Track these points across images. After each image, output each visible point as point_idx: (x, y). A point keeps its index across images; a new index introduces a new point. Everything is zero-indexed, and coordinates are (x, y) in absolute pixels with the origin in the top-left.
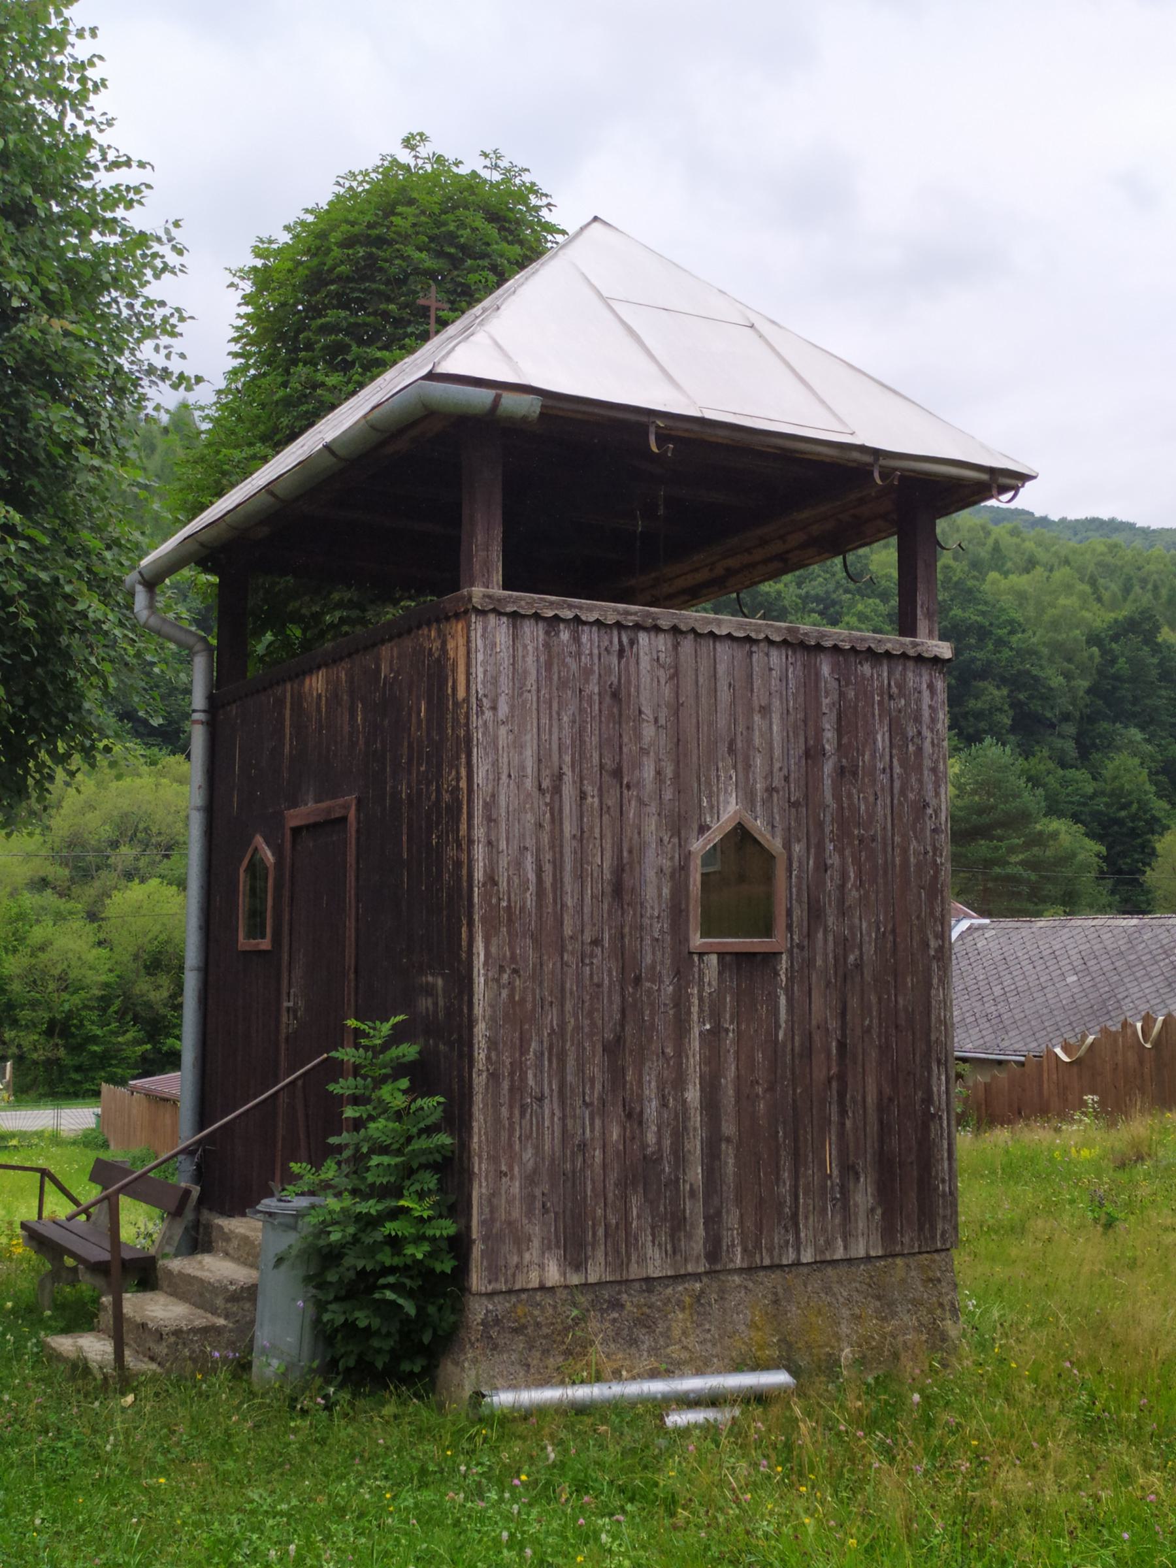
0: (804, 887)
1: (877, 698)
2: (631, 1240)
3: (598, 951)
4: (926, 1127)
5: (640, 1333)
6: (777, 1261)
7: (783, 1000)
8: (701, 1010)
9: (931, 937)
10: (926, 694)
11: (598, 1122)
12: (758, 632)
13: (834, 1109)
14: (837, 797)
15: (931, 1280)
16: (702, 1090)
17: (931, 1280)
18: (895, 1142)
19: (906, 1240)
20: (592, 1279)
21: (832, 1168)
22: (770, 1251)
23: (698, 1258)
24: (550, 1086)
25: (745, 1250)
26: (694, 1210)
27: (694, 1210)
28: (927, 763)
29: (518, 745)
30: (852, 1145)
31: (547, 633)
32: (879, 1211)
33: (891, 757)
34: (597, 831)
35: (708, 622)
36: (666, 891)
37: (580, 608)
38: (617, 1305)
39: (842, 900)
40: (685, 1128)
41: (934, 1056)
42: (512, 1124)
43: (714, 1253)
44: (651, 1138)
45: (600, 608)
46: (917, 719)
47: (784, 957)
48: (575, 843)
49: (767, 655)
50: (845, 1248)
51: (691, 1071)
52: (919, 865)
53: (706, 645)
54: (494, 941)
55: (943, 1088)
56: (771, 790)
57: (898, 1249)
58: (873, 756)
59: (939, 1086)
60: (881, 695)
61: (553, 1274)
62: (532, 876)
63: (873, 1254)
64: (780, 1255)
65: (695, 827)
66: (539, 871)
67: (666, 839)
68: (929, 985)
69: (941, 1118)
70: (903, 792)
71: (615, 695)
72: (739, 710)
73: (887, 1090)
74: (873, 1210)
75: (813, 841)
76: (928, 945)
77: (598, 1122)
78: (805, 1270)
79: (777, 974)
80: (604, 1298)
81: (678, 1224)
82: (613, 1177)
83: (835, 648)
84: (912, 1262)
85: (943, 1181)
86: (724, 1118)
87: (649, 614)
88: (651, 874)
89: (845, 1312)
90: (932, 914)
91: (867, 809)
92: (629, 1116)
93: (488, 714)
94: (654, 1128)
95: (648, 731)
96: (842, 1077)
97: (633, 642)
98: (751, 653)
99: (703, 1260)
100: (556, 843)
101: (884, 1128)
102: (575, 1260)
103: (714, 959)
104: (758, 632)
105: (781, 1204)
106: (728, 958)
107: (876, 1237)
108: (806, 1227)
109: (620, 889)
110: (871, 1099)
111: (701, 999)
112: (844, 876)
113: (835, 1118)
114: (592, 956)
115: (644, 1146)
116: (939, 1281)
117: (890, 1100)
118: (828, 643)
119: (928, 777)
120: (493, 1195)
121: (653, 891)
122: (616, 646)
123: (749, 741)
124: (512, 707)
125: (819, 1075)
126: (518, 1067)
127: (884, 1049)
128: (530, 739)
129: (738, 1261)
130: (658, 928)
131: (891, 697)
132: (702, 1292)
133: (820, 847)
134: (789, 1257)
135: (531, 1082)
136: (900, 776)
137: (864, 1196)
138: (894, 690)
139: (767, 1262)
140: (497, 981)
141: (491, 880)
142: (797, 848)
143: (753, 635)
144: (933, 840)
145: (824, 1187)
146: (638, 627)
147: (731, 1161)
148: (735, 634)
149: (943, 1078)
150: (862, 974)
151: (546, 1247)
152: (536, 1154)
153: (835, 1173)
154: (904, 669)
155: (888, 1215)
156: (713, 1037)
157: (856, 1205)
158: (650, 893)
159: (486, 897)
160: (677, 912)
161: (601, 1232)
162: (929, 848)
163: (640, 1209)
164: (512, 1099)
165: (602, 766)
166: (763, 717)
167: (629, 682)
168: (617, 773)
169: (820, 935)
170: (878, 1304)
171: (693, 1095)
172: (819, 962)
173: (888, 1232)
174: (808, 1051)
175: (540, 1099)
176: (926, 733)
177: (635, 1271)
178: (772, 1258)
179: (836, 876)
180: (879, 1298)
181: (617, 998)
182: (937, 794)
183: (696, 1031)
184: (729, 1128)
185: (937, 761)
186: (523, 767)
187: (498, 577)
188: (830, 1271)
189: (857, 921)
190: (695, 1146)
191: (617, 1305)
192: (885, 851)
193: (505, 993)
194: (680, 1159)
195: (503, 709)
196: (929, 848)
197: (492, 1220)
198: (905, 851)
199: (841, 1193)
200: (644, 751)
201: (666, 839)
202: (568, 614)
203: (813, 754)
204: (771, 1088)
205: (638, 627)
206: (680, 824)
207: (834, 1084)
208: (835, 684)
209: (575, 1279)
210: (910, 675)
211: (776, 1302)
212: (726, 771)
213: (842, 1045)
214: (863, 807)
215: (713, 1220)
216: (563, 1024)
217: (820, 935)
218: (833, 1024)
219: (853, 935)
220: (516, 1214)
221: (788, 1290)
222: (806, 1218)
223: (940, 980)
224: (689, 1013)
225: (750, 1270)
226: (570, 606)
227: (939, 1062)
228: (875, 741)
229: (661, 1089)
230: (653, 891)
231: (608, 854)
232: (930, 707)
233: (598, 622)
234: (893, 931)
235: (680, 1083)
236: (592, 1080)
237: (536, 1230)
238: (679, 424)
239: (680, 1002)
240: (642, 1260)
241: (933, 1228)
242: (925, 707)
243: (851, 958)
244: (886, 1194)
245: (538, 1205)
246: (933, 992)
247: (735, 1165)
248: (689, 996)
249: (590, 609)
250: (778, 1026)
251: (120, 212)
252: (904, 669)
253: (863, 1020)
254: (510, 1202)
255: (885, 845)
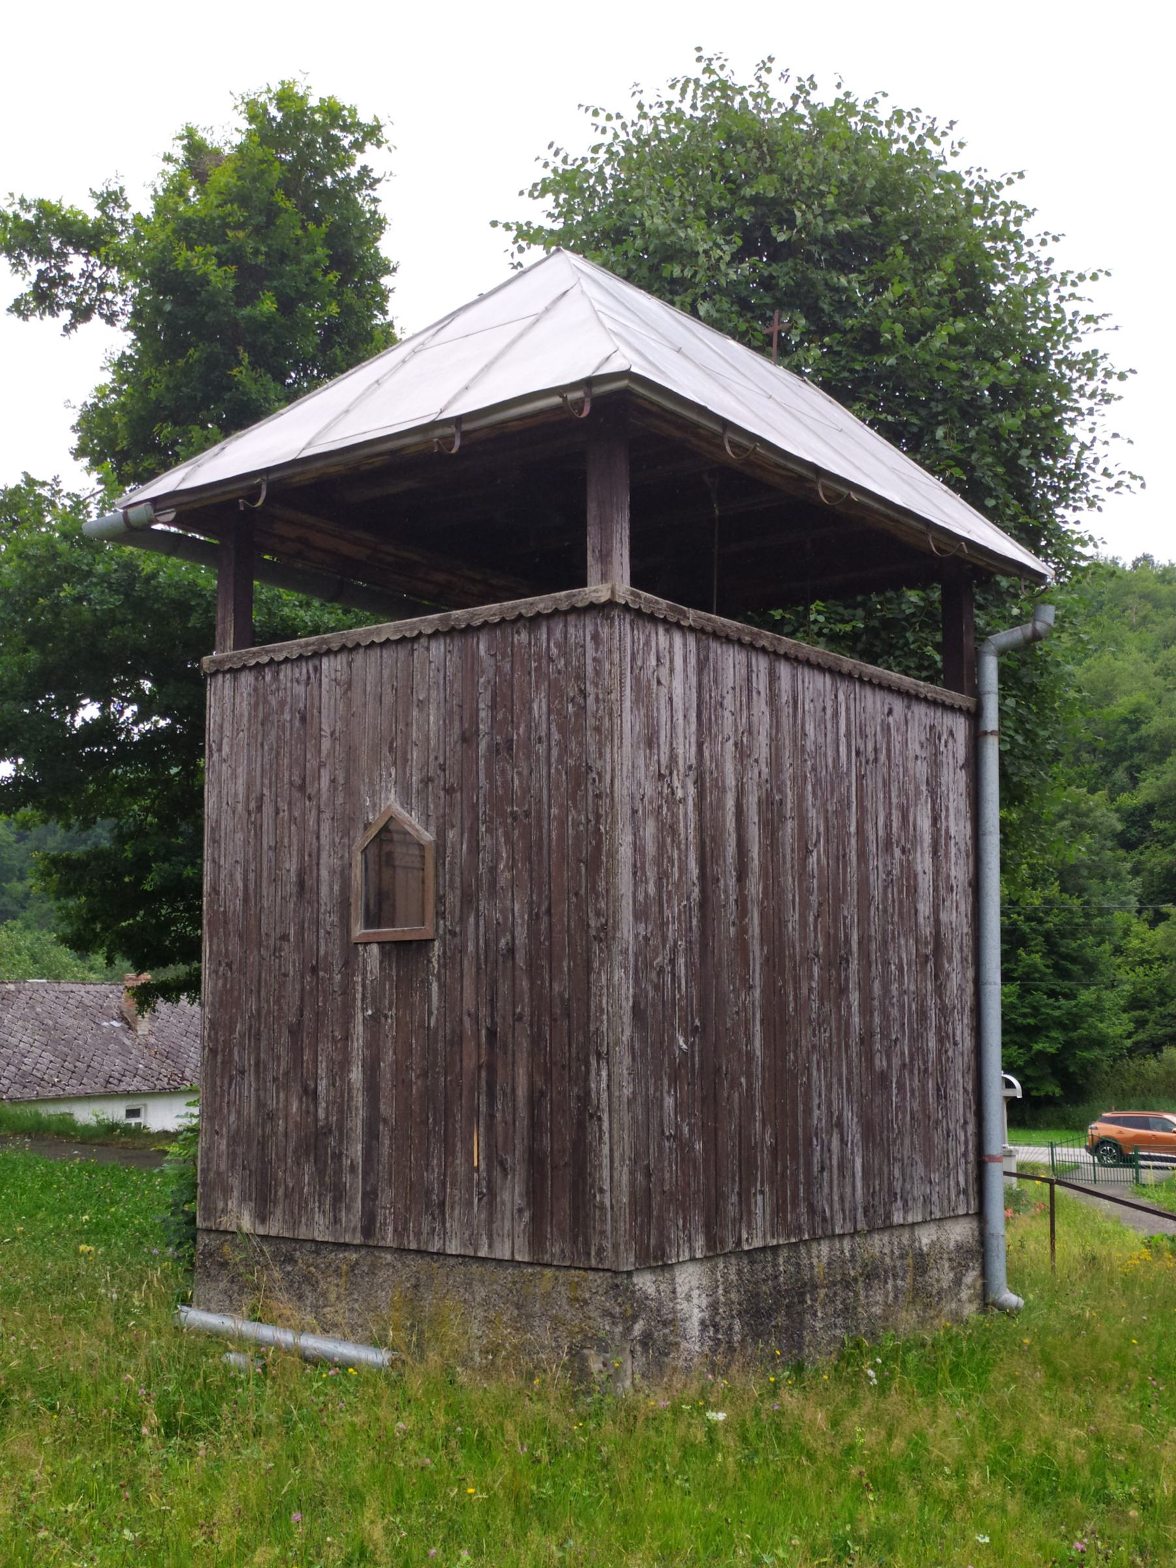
0: (457, 872)
1: (534, 664)
2: (303, 1206)
3: (285, 945)
4: (581, 1127)
5: (306, 1289)
6: (423, 1247)
7: (435, 987)
8: (364, 998)
9: (591, 915)
10: (590, 645)
11: (282, 1095)
12: (411, 630)
13: (483, 1099)
14: (490, 776)
15: (577, 1300)
16: (364, 1072)
17: (577, 1300)
18: (547, 1140)
19: (556, 1249)
20: (273, 1233)
21: (478, 1158)
22: (418, 1234)
23: (354, 1229)
24: (249, 1061)
25: (395, 1230)
26: (355, 1185)
27: (355, 1185)
28: (591, 722)
29: (234, 776)
30: (500, 1139)
31: (256, 679)
32: (527, 1215)
33: (549, 724)
34: (286, 840)
35: (370, 633)
36: (336, 888)
37: (273, 651)
38: (291, 1260)
39: (493, 883)
40: (349, 1107)
41: (592, 1048)
42: (222, 1091)
43: (368, 1229)
44: (321, 1114)
45: (287, 647)
46: (580, 677)
47: (436, 944)
48: (271, 853)
49: (428, 649)
50: (490, 1246)
51: (355, 1053)
52: (578, 837)
53: (375, 654)
54: (215, 940)
55: (604, 1085)
56: (427, 781)
57: (547, 1258)
58: (529, 728)
59: (599, 1082)
60: (539, 661)
61: (246, 1224)
62: (240, 885)
63: (518, 1258)
64: (427, 1243)
65: (361, 826)
66: (246, 880)
67: (337, 840)
68: (588, 969)
69: (600, 1119)
70: (560, 760)
71: (303, 719)
72: (400, 709)
73: (540, 1083)
74: (520, 1211)
75: (467, 824)
76: (588, 926)
77: (282, 1095)
78: (452, 1261)
79: (429, 961)
80: (285, 1249)
81: (340, 1196)
82: (292, 1144)
83: (485, 624)
84: (561, 1274)
85: (602, 1191)
86: (382, 1100)
87: (324, 641)
88: (324, 873)
89: (480, 1313)
90: (594, 888)
91: (521, 782)
92: (305, 1090)
93: (216, 755)
94: (324, 1105)
95: (326, 744)
96: (491, 1068)
97: (317, 669)
98: (413, 650)
99: (358, 1234)
100: (258, 856)
101: (535, 1125)
102: (262, 1217)
103: (375, 949)
104: (411, 630)
105: (428, 1193)
106: (387, 947)
107: (521, 1242)
108: (451, 1217)
109: (304, 887)
110: (522, 1092)
111: (364, 986)
112: (497, 856)
113: (483, 1108)
114: (281, 949)
115: (316, 1119)
116: (586, 1302)
117: (542, 1094)
118: (477, 622)
119: (591, 738)
120: (209, 1149)
121: (328, 889)
122: (304, 676)
123: (407, 736)
124: (231, 747)
125: (469, 1063)
126: (228, 1044)
127: (536, 1040)
128: (242, 771)
129: (389, 1240)
130: (330, 919)
131: (551, 659)
132: (357, 1263)
133: (474, 831)
134: (435, 1246)
135: (236, 1058)
136: (558, 743)
137: (512, 1193)
138: (554, 651)
139: (413, 1246)
140: (216, 972)
141: (215, 890)
142: (451, 834)
143: (408, 635)
144: (596, 806)
145: (471, 1180)
146: (317, 655)
147: (387, 1142)
148: (393, 638)
149: (604, 1073)
150: (513, 959)
151: (244, 1199)
152: (238, 1118)
153: (483, 1167)
154: (566, 626)
155: (537, 1222)
156: (373, 1023)
157: (503, 1203)
158: (324, 890)
159: (211, 903)
160: (344, 905)
161: (281, 1192)
162: (591, 817)
163: (312, 1178)
164: (223, 1069)
165: (291, 783)
166: (421, 710)
167: (312, 705)
168: (302, 788)
169: (472, 920)
170: (516, 1312)
171: (356, 1075)
172: (471, 948)
173: (536, 1240)
174: (457, 1040)
175: (243, 1073)
176: (590, 689)
177: (303, 1233)
178: (419, 1242)
179: (488, 858)
180: (518, 1306)
181: (298, 987)
182: (601, 755)
183: (359, 1017)
184: (387, 1109)
185: (601, 719)
186: (236, 795)
187: (230, 642)
188: (474, 1268)
189: (509, 903)
190: (357, 1123)
191: (291, 1260)
192: (541, 828)
193: (220, 983)
194: (343, 1135)
195: (226, 749)
196: (591, 817)
197: (208, 1169)
198: (562, 823)
199: (488, 1188)
200: (322, 765)
201: (337, 840)
202: (265, 659)
203: (468, 739)
204: (424, 1074)
205: (317, 655)
206: (347, 823)
207: (484, 1074)
208: (492, 661)
209: (261, 1231)
210: (572, 630)
211: (416, 1287)
212: (388, 769)
213: (492, 1034)
214: (516, 782)
215: (370, 1196)
216: (259, 1010)
217: (472, 920)
218: (484, 1011)
219: (505, 918)
220: (223, 1167)
221: (431, 1277)
222: (452, 1208)
223: (602, 963)
224: (354, 999)
225: (401, 1251)
226: (267, 652)
227: (599, 1055)
228: (531, 709)
229: (330, 1070)
230: (328, 889)
231: (295, 860)
232: (595, 659)
233: (286, 660)
234: (549, 911)
235: (344, 1065)
236: (279, 1058)
237: (235, 1182)
238: (319, 464)
239: (347, 990)
240: (310, 1223)
241: (587, 1244)
242: (589, 661)
243: (503, 942)
244: (535, 1196)
245: (239, 1161)
246: (593, 977)
247: (390, 1147)
248: (355, 983)
249: (281, 650)
250: (430, 1013)
251: (715, 315)
252: (566, 626)
253: (514, 1008)
254: (219, 1156)
255: (539, 819)
